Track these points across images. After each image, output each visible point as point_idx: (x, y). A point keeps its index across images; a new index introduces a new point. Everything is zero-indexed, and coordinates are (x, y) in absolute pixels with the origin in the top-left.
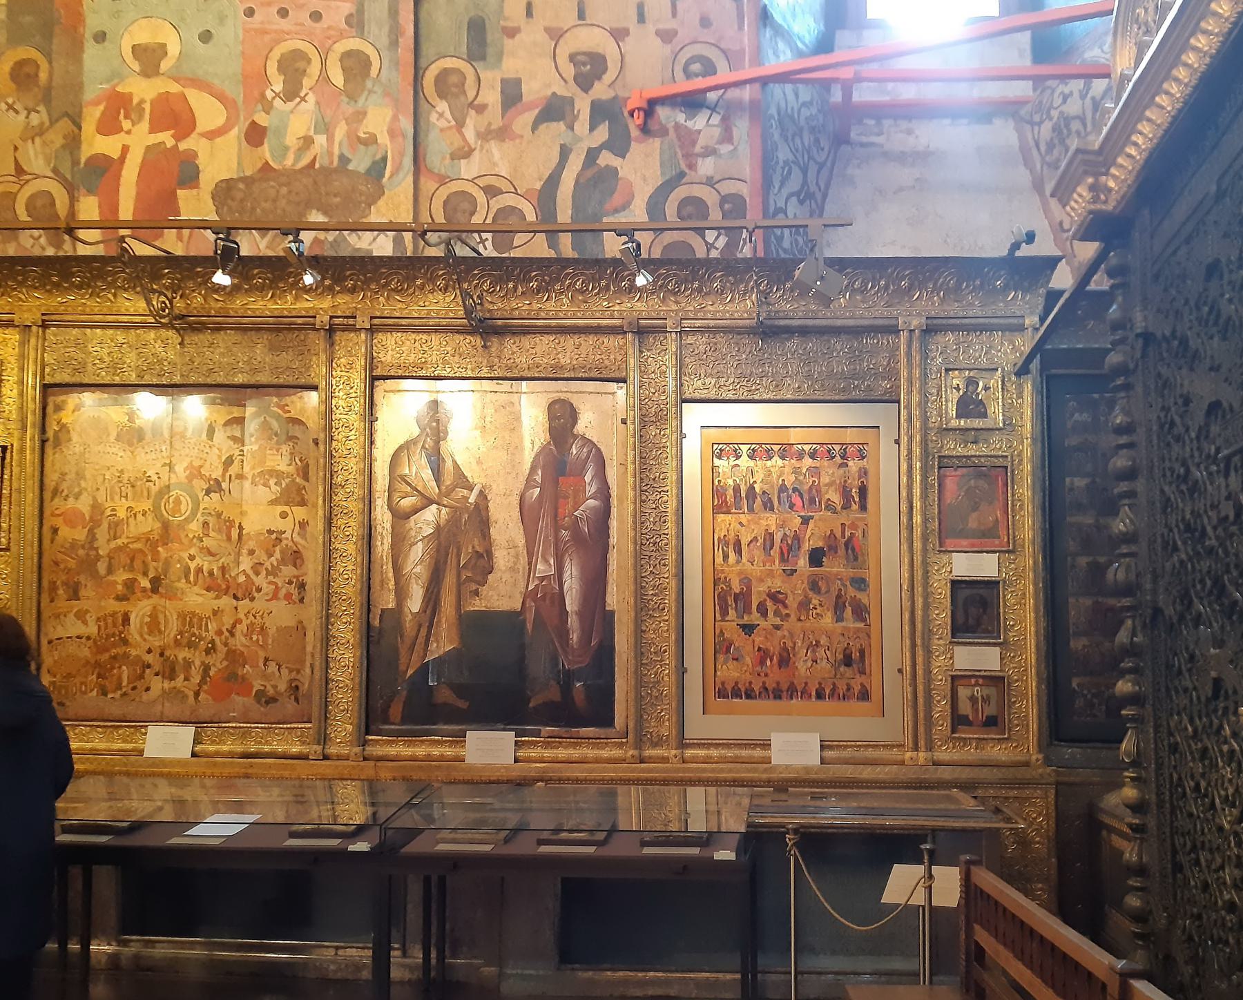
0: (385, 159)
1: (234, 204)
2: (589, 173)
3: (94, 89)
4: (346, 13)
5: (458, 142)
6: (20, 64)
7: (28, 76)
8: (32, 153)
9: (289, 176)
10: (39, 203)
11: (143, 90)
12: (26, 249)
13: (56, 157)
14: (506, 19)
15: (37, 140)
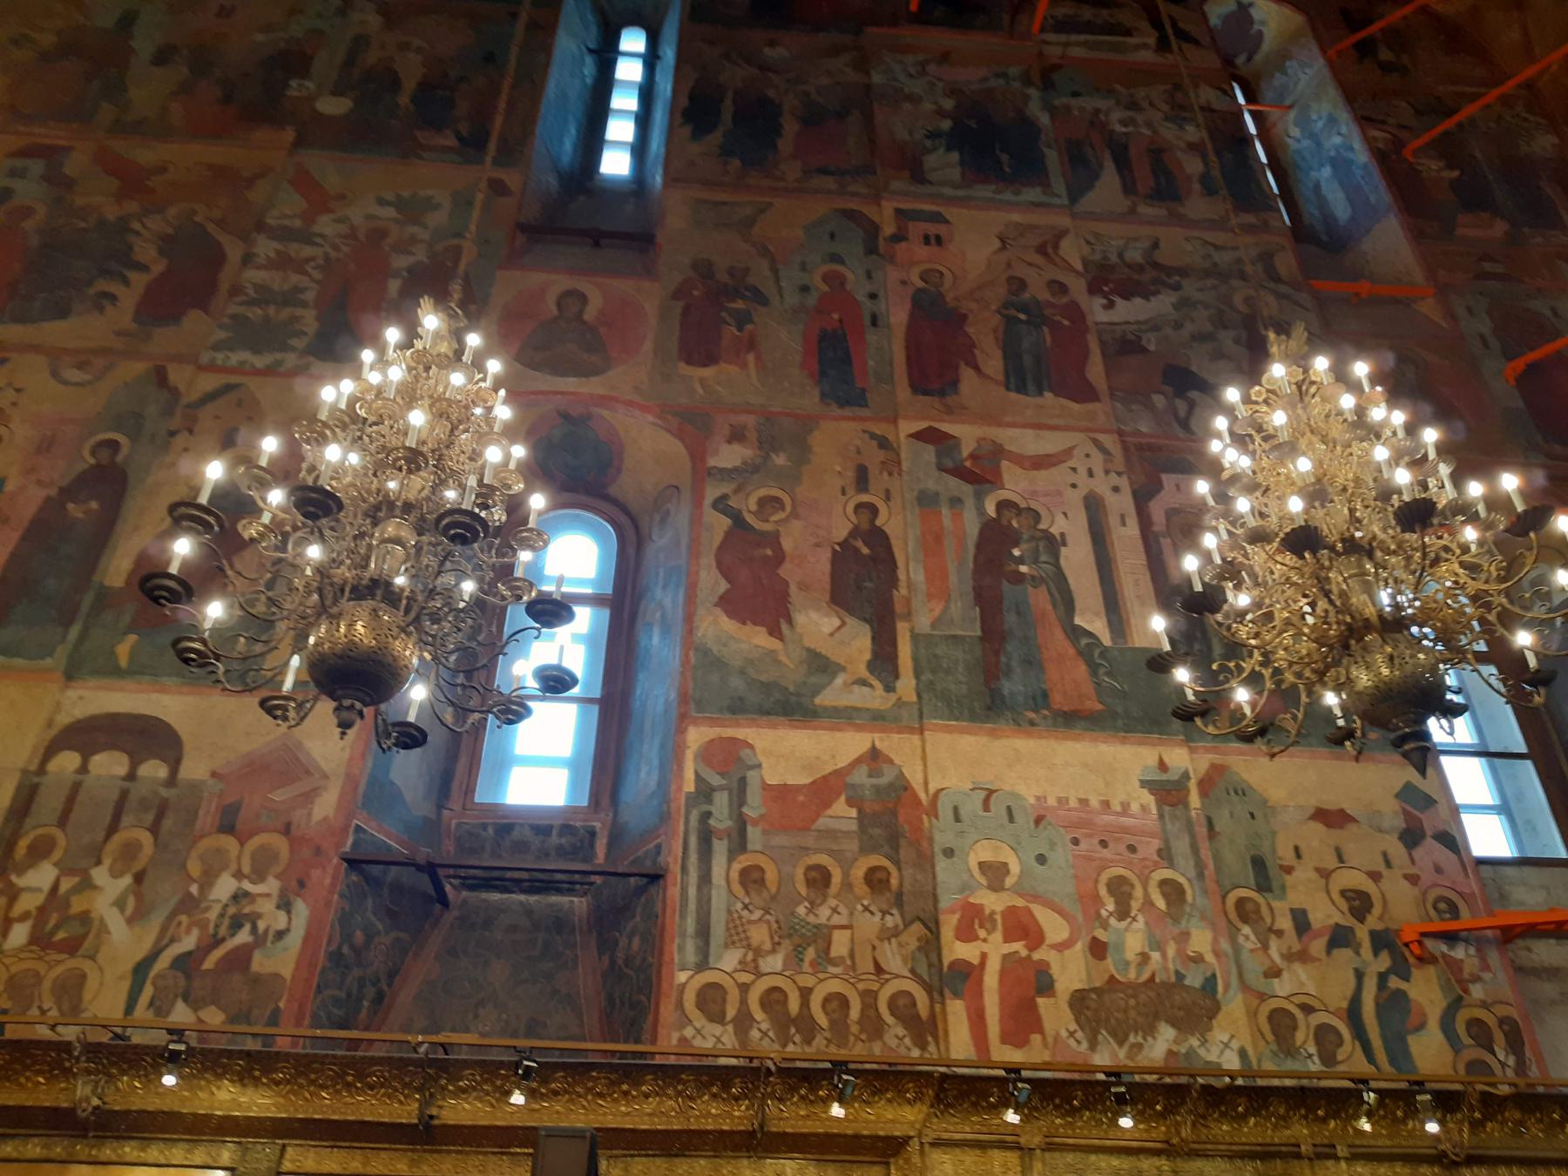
0: (1214, 975)
1: (1089, 1014)
2: (1385, 995)
3: (948, 899)
4: (1157, 847)
5: (1267, 964)
6: (872, 871)
7: (880, 881)
8: (889, 953)
9: (1133, 989)
10: (901, 1002)
11: (993, 902)
12: (891, 1048)
13: (913, 959)
14: (1281, 859)
15: (893, 940)
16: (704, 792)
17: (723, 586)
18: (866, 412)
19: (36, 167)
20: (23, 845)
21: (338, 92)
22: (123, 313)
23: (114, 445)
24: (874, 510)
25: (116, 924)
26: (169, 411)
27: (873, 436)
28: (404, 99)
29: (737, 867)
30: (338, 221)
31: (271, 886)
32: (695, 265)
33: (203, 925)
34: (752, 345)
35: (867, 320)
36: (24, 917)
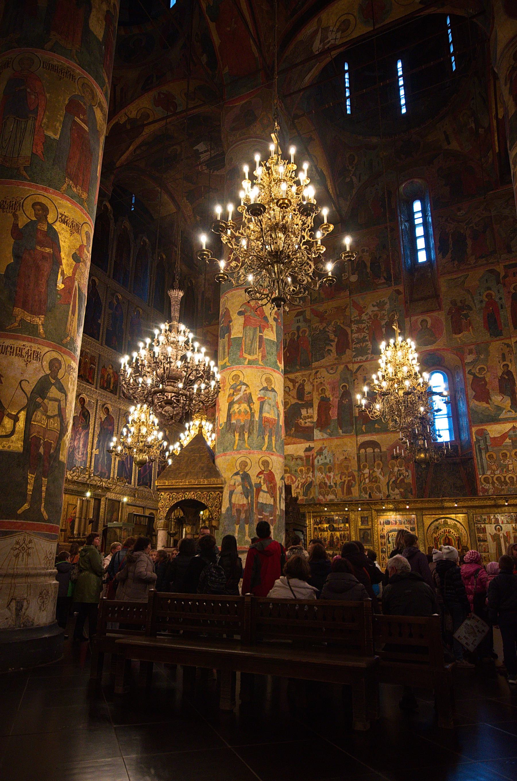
16: (478, 441)
17: (474, 393)
18: (502, 337)
19: (301, 318)
20: (362, 466)
21: (353, 274)
22: (334, 354)
23: (344, 386)
24: (508, 366)
25: (381, 477)
26: (352, 376)
27: (505, 344)
28: (369, 270)
29: (487, 455)
30: (366, 315)
31: (403, 468)
32: (451, 303)
33: (395, 475)
34: (470, 324)
35: (500, 307)
36: (367, 478)
